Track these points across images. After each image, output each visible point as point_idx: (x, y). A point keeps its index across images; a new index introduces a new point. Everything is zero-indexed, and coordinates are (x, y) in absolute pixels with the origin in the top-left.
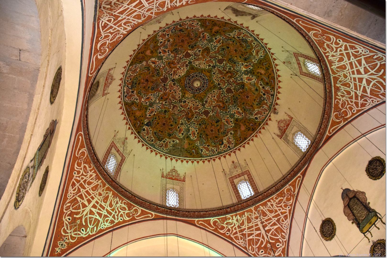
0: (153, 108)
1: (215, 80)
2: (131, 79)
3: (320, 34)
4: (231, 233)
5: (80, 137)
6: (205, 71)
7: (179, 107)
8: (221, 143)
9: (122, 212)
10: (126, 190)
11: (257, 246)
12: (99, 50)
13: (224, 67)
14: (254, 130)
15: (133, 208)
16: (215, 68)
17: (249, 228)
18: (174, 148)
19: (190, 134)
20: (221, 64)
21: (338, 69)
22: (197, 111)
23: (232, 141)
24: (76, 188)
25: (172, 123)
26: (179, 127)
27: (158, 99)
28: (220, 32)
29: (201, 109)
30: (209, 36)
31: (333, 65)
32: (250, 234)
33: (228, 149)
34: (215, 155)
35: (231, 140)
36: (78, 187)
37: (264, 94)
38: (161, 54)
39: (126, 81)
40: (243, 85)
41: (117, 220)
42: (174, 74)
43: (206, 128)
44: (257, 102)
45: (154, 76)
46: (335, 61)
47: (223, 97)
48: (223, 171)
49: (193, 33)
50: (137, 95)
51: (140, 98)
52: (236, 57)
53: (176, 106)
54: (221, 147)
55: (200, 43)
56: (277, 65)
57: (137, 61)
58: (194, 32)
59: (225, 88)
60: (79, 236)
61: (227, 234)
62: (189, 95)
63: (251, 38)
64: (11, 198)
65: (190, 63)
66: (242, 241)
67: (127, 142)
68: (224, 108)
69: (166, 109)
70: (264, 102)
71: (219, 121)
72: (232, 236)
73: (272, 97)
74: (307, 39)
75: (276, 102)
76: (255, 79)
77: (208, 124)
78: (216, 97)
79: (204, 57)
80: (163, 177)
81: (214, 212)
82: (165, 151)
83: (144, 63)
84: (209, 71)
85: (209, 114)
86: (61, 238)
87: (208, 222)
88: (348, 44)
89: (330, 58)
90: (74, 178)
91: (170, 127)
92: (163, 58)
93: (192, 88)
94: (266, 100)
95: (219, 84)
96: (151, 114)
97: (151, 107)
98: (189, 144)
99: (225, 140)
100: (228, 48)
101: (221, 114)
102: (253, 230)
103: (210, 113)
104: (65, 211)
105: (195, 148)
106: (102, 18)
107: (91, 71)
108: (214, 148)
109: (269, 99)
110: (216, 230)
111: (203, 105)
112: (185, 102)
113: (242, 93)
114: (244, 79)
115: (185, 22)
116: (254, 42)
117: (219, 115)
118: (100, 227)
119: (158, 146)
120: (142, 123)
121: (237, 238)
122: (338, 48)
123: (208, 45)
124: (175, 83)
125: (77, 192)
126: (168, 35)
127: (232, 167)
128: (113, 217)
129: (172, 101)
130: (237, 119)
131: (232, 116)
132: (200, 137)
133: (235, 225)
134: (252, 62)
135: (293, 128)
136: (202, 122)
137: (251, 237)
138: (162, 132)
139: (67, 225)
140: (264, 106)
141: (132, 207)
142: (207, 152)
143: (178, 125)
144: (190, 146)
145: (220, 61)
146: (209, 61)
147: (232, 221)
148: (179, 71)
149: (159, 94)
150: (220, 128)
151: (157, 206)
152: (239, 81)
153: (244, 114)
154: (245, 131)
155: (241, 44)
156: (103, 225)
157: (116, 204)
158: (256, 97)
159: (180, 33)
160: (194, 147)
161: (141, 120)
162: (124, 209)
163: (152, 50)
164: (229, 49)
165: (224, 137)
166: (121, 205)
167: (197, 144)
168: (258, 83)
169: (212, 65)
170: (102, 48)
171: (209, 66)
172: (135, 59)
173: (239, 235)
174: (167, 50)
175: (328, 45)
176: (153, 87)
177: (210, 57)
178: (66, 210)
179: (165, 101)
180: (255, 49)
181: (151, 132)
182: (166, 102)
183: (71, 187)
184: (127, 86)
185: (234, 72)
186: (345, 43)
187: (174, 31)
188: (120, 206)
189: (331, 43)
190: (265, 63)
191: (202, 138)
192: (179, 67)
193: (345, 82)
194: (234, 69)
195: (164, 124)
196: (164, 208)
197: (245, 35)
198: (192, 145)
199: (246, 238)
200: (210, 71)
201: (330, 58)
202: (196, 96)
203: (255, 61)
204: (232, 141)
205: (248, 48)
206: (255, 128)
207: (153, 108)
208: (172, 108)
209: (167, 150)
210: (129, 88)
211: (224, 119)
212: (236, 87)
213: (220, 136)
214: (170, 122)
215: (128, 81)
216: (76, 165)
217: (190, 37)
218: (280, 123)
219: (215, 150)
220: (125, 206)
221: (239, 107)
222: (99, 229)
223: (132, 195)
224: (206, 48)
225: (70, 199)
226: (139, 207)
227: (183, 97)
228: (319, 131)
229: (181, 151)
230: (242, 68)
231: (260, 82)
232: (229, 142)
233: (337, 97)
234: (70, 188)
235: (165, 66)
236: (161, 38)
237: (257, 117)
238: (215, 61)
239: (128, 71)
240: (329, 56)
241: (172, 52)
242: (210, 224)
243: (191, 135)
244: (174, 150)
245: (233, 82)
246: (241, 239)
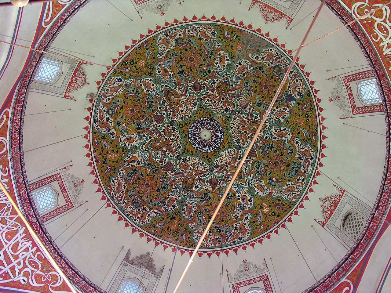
0: (276, 118)
1: (178, 137)
2: (298, 180)
3: (50, 282)
6: (192, 152)
7: (237, 104)
8: (180, 41)
10: (365, 49)
13: (164, 157)
14: (125, 62)
15: (365, 20)
16: (178, 156)
18: (259, 49)
19: (228, 60)
20: (168, 162)
21: (16, 229)
22: (210, 92)
23: (161, 43)
25: (254, 85)
26: (244, 75)
27: (266, 127)
28: (168, 218)
29: (204, 93)
30: (183, 212)
31: (24, 233)
33: (169, 32)
34: (192, 25)
35: (162, 44)
37: (108, 119)
38: (249, 198)
39: (305, 181)
40: (138, 130)
42: (237, 158)
43: (201, 65)
44: (118, 106)
45: (266, 166)
46: (22, 243)
47: (169, 109)
48: (182, 3)
49: (204, 220)
50: (295, 150)
51: (291, 141)
52: (147, 175)
53: (242, 108)
54: (180, 35)
55: (195, 201)
56: (92, 173)
57: (283, 205)
58: (202, 222)
59: (164, 124)
62: (220, 119)
63: (128, 211)
65: (211, 170)
67: (332, 95)
68: (169, 92)
69: (259, 108)
70: (107, 107)
71: (178, 73)
73: (96, 119)
74: (63, 261)
75: (89, 113)
76: (121, 141)
77: (197, 70)
78: (179, 110)
79: (190, 176)
80: (289, 18)
82: (275, 49)
83: (274, 194)
84: (186, 151)
85: (192, 85)
88: (13, 279)
89: (29, 244)
91: (257, 79)
92: (247, 189)
93: (215, 130)
94: (105, 111)
95: (173, 129)
96: (282, 110)
97: (279, 120)
98: (232, 47)
99: (172, 45)
100: (158, 190)
101: (175, 83)
103: (192, 86)
105: (224, 40)
108: (193, 35)
109: (101, 114)
111: (200, 99)
112: (227, 110)
113: (141, 116)
114: (137, 139)
115: (213, 245)
116: (124, 204)
117: (178, 82)
119: (285, 61)
120: (299, 104)
122: (24, 268)
123: (184, 196)
124: (238, 143)
126: (236, 229)
127: (165, 8)
129: (246, 117)
130: (150, 76)
131: (157, 80)
132: (212, 54)
134: (126, 168)
135: (63, 82)
136: (205, 74)
138: (272, 78)
140: (108, 102)
141: (365, 22)
142: (205, 30)
143: (244, 79)
144: (231, 44)
145: (169, 166)
146: (185, 169)
148: (228, 159)
149: (264, 135)
150: (178, 63)
152: (144, 135)
153: (139, 85)
154: (138, 59)
155: (141, 197)
158: (120, 112)
159: (220, 226)
160: (225, 42)
161: (299, 109)
163: (260, 211)
164: (157, 188)
165: (173, 50)
167: (220, 44)
168: (116, 137)
169: (182, 160)
171: (185, 160)
172: (285, 209)
174: (240, 201)
175: (37, 267)
176: (270, 149)
177: (183, 174)
179: (257, 121)
180: (123, 191)
181: (288, 85)
182: (256, 118)
184: (305, 172)
185: (150, 150)
186: (16, 279)
187: (228, 235)
189: (34, 271)
190: (108, 171)
191: (210, 51)
192: (227, 167)
193: (2, 212)
194: (151, 154)
195: (266, 87)
197: (136, 215)
198: (228, 45)
200: (185, 151)
201: (29, 244)
202: (210, 115)
203: (122, 170)
204: (161, 43)
205: (132, 193)
206: (122, 64)
207: (276, 118)
208: (249, 107)
209: (271, 50)
210: (304, 167)
211: (170, 75)
212: (149, 126)
213: (180, 51)
214: (256, 87)
215: (303, 180)
217: (208, 215)
218: (83, 83)
219: (191, 32)
220: (377, 31)
221: (146, 95)
223: (356, 35)
224: (188, 191)
227: (228, 118)
228: (22, 107)
229: (248, 41)
230: (139, 156)
231: (115, 138)
232: (166, 42)
233: (7, 180)
235: (248, 174)
236: (245, 226)
237: (118, 83)
238: (176, 168)
239: (300, 195)
240: (32, 248)
241: (234, 195)
243: (226, 59)
244: (260, 46)
245: (153, 133)
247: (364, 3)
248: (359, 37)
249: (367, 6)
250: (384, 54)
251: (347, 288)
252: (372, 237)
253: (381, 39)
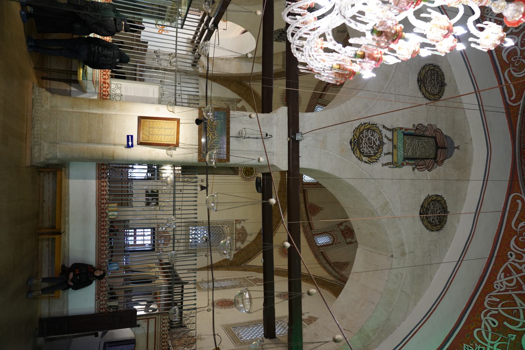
5: (519, 201)
12: (508, 62)
86: (472, 343)
106: (488, 14)
107: (510, 96)
139: (486, 328)
170: (512, 59)
183: (503, 274)
216: (512, 243)
225: (499, 292)
234: (501, 274)
251: (512, 99)
252: (521, 151)
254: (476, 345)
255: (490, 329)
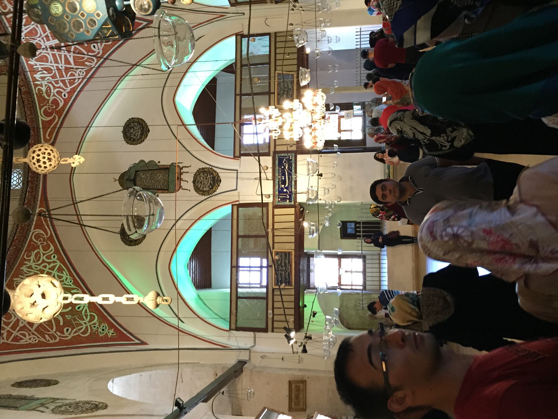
4: (65, 90)
9: (43, 258)
11: (85, 53)
17: (56, 62)
24: (20, 334)
32: (65, 61)
36: (19, 331)
41: (56, 262)
60: (88, 311)
61: (65, 95)
64: (103, 416)
66: (77, 75)
72: (68, 89)
81: (28, 113)
86: (95, 333)
87: (47, 125)
90: (5, 341)
102: (58, 54)
104: (57, 340)
110: (59, 113)
118: (70, 285)
121: (72, 82)
125: (26, 331)
128: (53, 270)
133: (51, 83)
137: (71, 60)
139: (76, 332)
147: (44, 86)
151: (24, 204)
156: (67, 281)
157: (32, 268)
162: (38, 255)
166: (32, 261)
173: (67, 78)
178: (55, 338)
183: (20, 341)
188: (34, 261)
196: (26, 194)
199: (73, 68)
220: (33, 254)
222: (73, 286)
225: (38, 337)
226: (31, 233)
234: (22, 342)
242: (51, 122)
246: (74, 76)
247: (45, 235)
248: (11, 248)
249: (45, 238)
250: (21, 268)
253: (31, 259)
254: (94, 331)
255: (75, 330)
